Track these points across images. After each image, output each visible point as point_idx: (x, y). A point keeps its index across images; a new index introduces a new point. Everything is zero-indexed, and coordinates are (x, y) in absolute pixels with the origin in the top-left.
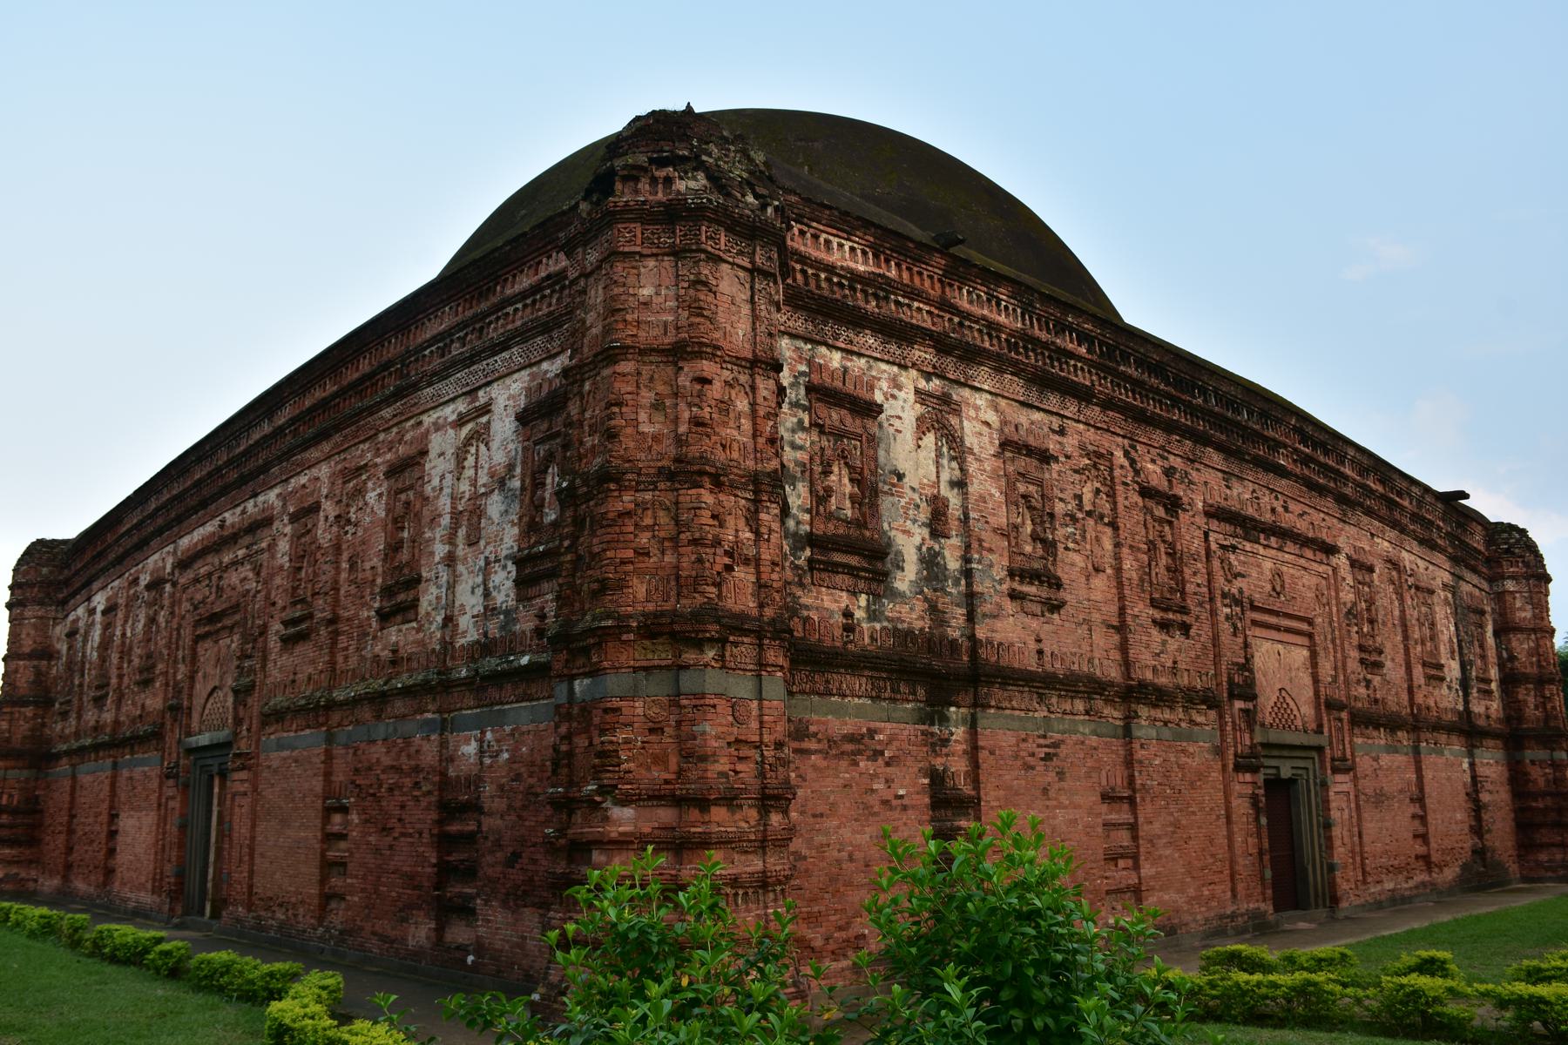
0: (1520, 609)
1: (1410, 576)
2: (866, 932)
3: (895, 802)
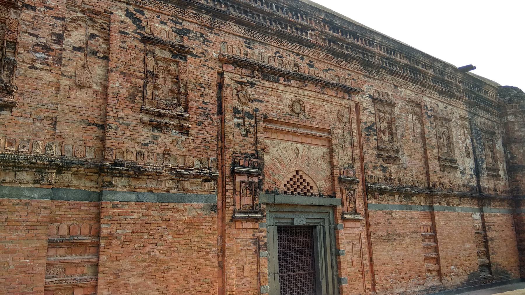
0: (517, 131)
1: (431, 110)
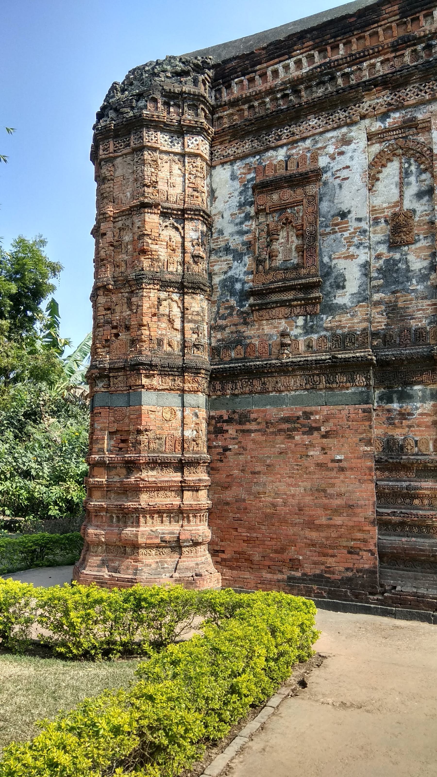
2: (301, 558)
3: (330, 465)
